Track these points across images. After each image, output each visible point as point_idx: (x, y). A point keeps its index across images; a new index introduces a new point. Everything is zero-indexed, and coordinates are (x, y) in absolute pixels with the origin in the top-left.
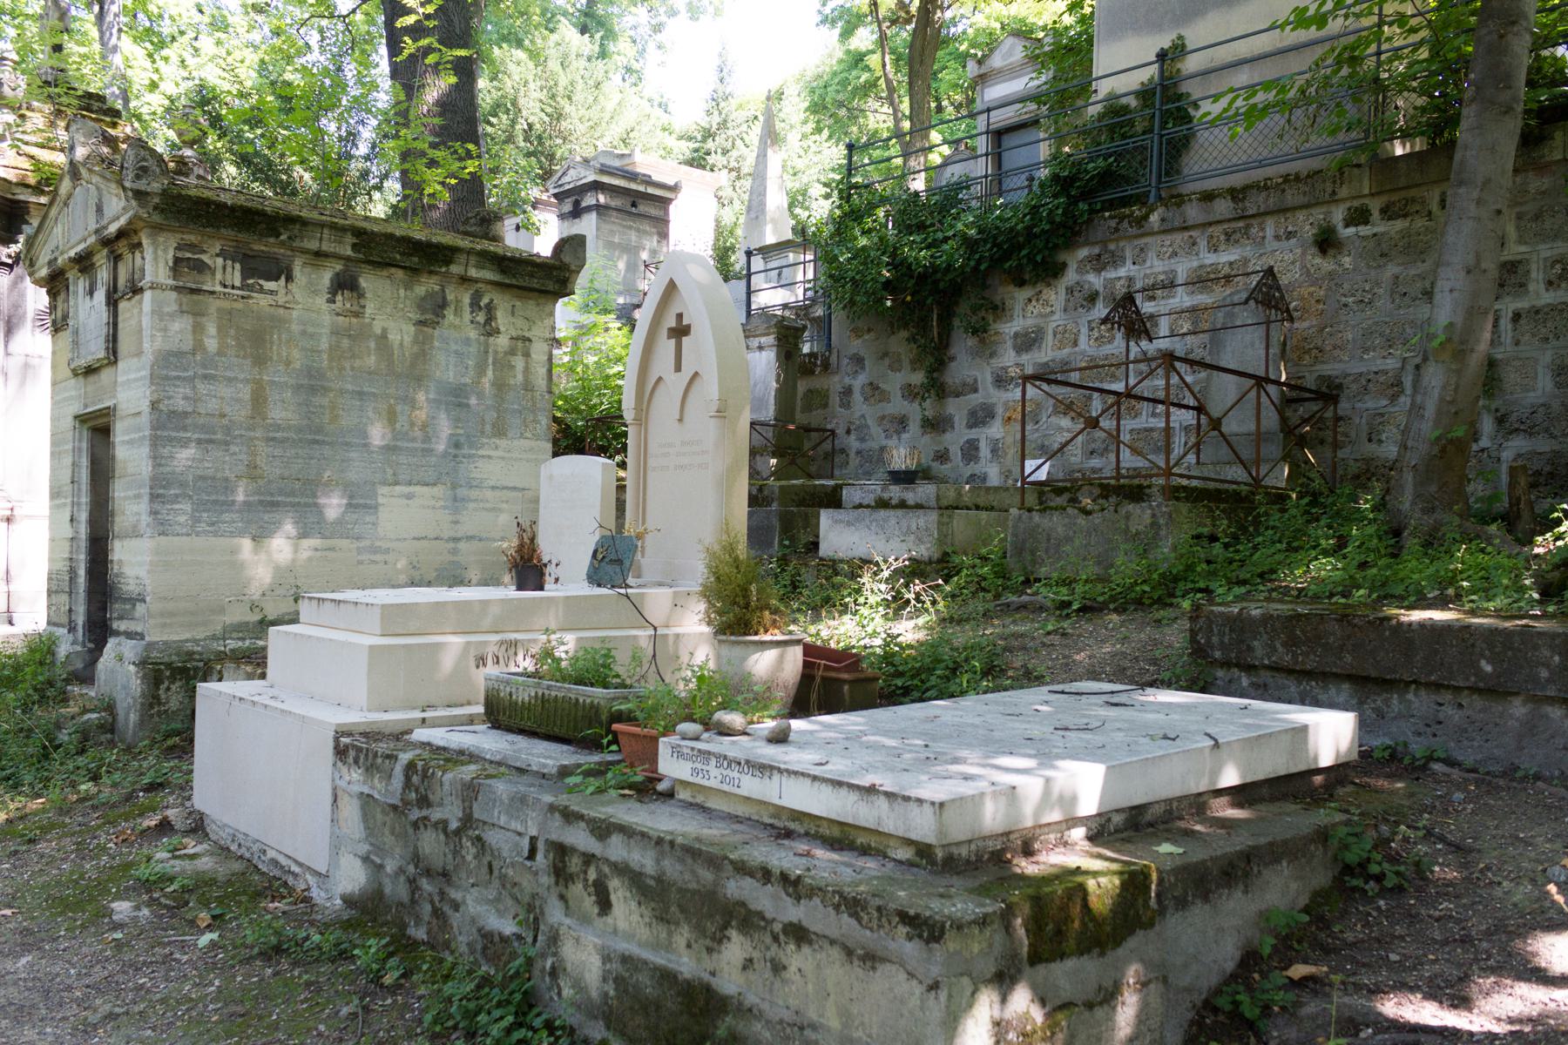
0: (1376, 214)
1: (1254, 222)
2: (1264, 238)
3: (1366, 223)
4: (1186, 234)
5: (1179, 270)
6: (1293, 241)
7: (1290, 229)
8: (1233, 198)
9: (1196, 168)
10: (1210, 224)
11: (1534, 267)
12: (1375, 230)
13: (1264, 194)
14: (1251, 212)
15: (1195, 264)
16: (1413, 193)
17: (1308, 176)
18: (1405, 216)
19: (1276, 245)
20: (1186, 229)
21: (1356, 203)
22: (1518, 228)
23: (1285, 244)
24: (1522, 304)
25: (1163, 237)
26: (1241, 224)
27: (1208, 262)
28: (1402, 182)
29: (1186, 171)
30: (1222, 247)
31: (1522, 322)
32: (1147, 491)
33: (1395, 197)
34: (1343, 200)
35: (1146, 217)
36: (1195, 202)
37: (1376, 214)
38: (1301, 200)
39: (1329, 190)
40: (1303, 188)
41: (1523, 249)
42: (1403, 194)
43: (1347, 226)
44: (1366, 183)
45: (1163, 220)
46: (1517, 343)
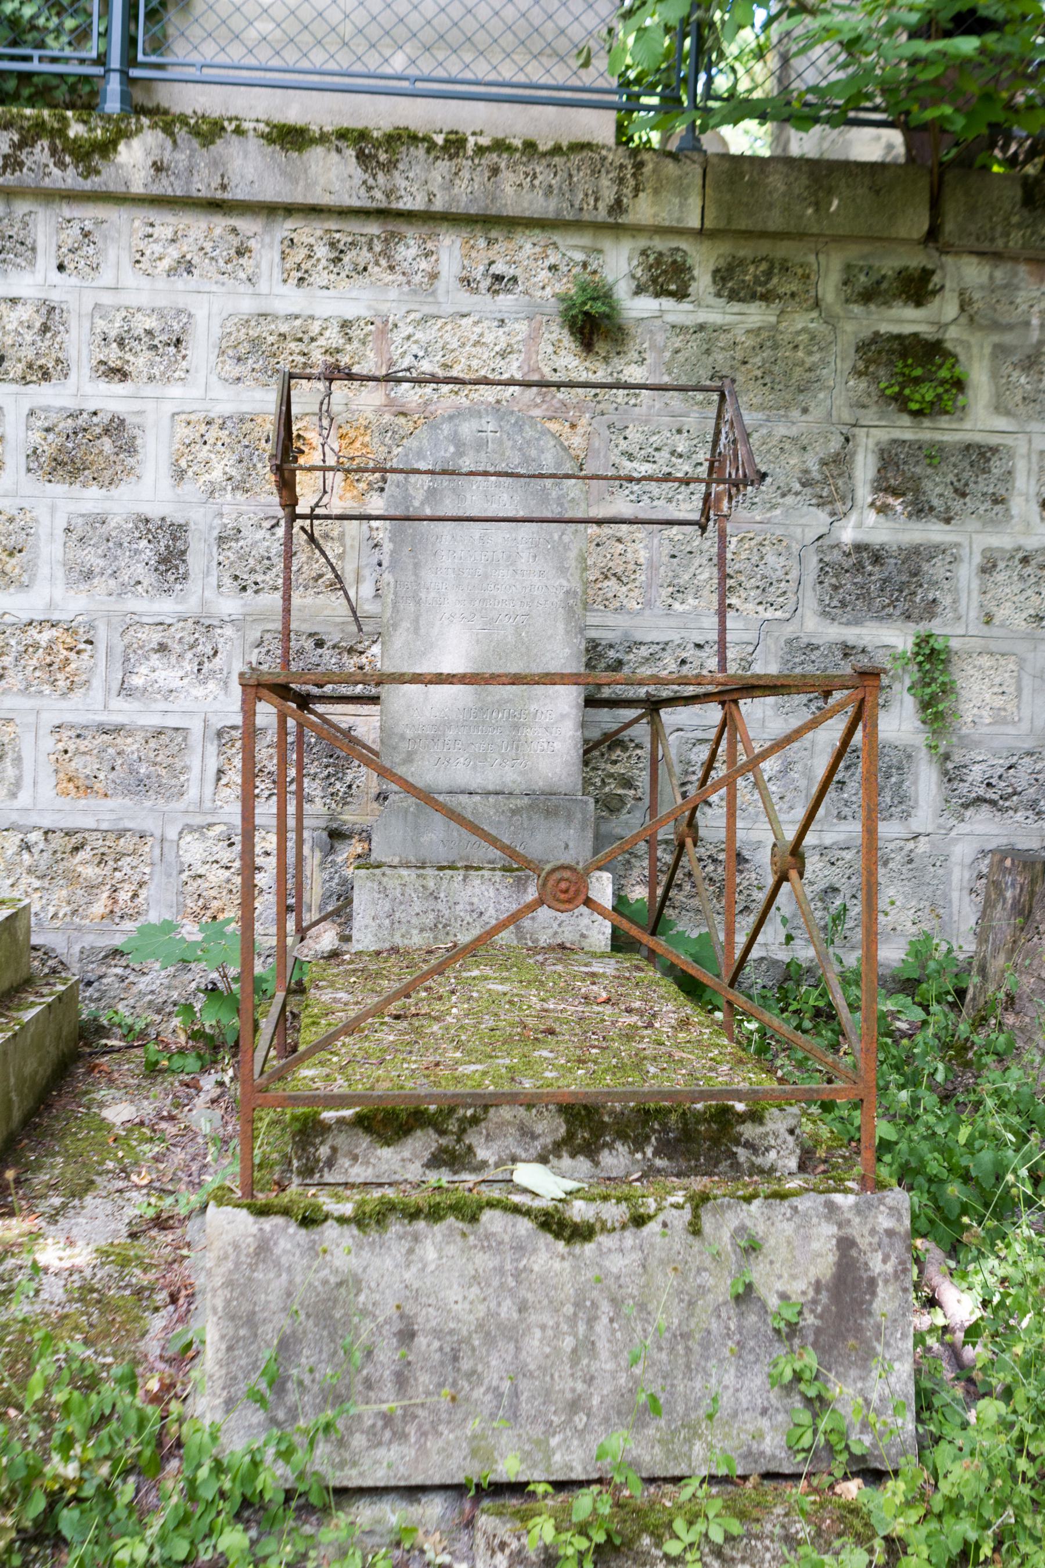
0: (702, 282)
1: (411, 233)
2: (434, 276)
3: (681, 295)
4: (220, 223)
5: (200, 315)
6: (505, 301)
7: (499, 268)
8: (362, 158)
9: (209, 51)
10: (290, 210)
11: (1021, 466)
12: (704, 316)
13: (444, 166)
14: (406, 204)
15: (247, 306)
16: (782, 250)
17: (557, 150)
18: (766, 298)
19: (464, 300)
20: (215, 206)
21: (660, 244)
22: (995, 375)
23: (484, 302)
24: (1002, 540)
25: (153, 215)
26: (373, 228)
27: (282, 307)
28: (775, 221)
29: (180, 51)
30: (320, 277)
31: (1000, 577)
32: (748, 1131)
33: (745, 251)
34: (636, 230)
35: (106, 148)
36: (253, 144)
37: (702, 282)
38: (535, 204)
39: (609, 195)
40: (545, 176)
41: (1002, 423)
42: (765, 248)
43: (639, 290)
44: (694, 203)
45: (158, 168)
46: (989, 619)
